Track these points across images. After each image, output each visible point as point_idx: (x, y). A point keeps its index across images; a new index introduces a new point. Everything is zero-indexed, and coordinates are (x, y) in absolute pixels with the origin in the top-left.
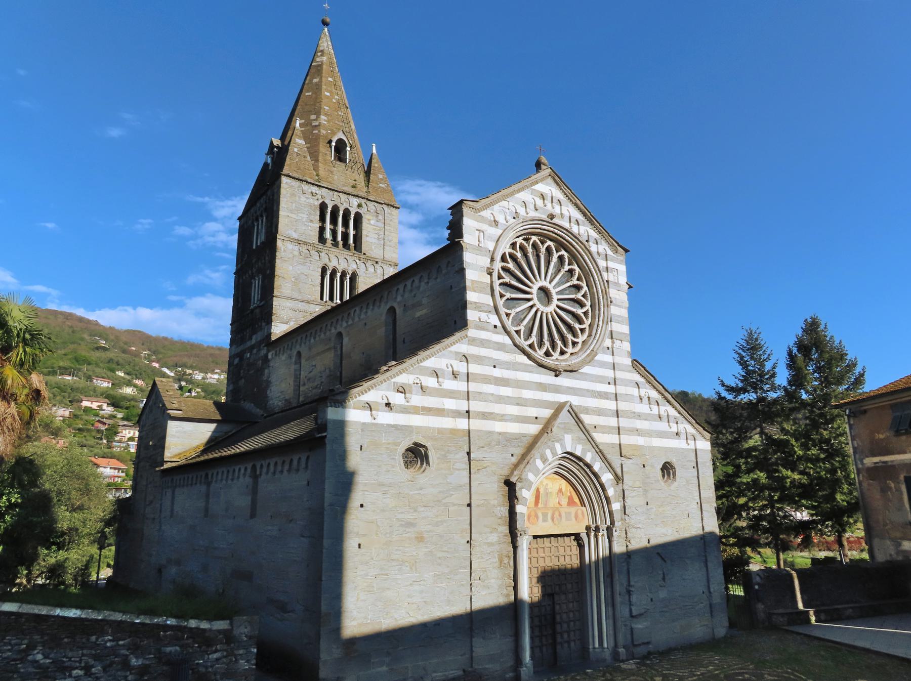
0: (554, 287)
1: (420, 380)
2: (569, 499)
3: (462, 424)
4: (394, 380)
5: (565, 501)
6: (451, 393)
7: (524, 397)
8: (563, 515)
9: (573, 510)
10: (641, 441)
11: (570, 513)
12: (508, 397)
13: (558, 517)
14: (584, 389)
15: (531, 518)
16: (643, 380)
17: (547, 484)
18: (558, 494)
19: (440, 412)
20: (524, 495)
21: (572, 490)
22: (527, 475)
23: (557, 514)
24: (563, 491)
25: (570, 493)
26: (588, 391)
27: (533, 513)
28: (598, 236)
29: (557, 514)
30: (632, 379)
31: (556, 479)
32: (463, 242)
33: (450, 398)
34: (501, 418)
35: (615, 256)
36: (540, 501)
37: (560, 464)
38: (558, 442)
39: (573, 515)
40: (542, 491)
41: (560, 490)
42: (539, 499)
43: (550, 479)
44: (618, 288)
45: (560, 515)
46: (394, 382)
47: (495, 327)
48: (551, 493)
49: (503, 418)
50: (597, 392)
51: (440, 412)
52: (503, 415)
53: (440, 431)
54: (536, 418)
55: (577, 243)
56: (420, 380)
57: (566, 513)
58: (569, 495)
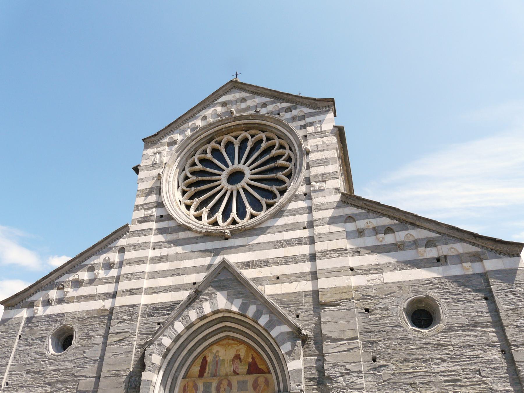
0: (233, 163)
1: (78, 276)
2: (250, 365)
3: (108, 304)
4: (56, 281)
5: (243, 368)
6: (105, 279)
7: (181, 267)
8: (235, 384)
9: (251, 378)
10: (356, 281)
11: (245, 382)
12: (163, 271)
13: (226, 387)
14: (265, 243)
15: (188, 390)
16: (361, 211)
17: (218, 351)
18: (233, 360)
19: (91, 297)
20: (153, 361)
21: (255, 355)
22: (161, 339)
23: (225, 383)
24: (242, 357)
25: (253, 358)
26: (270, 243)
27: (191, 384)
28: (291, 105)
29: (225, 383)
30: (342, 214)
31: (231, 344)
32: (140, 166)
33: (105, 283)
34: (152, 291)
35: (317, 110)
36: (207, 371)
37: (225, 326)
38: (206, 300)
39: (250, 385)
40: (210, 359)
41: (237, 357)
42: (205, 369)
43: (223, 345)
44: (320, 136)
45: (230, 384)
46: (57, 282)
47: (162, 216)
48: (223, 360)
49: (155, 290)
50: (285, 241)
51: (91, 297)
52: (154, 288)
53: (88, 312)
54: (195, 284)
55: (267, 121)
56: (78, 276)
57: (238, 382)
58: (251, 360)
